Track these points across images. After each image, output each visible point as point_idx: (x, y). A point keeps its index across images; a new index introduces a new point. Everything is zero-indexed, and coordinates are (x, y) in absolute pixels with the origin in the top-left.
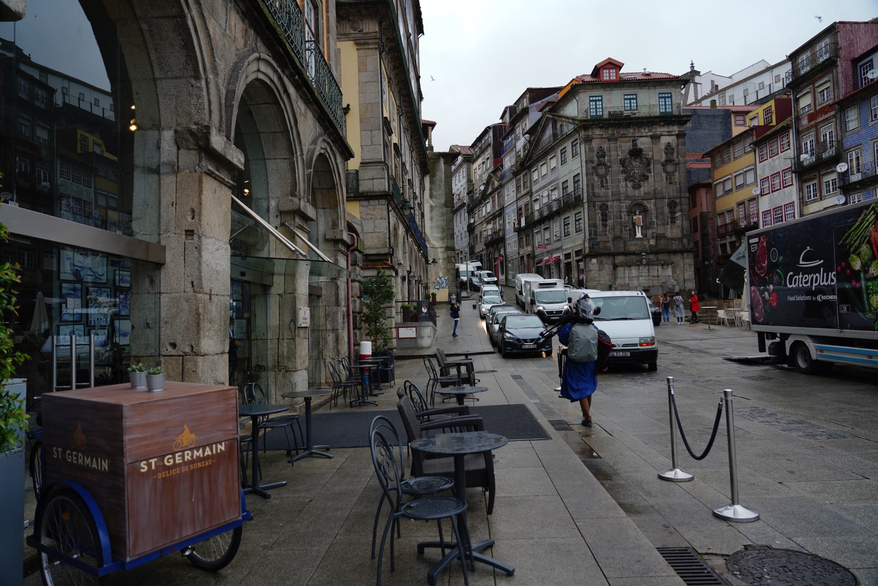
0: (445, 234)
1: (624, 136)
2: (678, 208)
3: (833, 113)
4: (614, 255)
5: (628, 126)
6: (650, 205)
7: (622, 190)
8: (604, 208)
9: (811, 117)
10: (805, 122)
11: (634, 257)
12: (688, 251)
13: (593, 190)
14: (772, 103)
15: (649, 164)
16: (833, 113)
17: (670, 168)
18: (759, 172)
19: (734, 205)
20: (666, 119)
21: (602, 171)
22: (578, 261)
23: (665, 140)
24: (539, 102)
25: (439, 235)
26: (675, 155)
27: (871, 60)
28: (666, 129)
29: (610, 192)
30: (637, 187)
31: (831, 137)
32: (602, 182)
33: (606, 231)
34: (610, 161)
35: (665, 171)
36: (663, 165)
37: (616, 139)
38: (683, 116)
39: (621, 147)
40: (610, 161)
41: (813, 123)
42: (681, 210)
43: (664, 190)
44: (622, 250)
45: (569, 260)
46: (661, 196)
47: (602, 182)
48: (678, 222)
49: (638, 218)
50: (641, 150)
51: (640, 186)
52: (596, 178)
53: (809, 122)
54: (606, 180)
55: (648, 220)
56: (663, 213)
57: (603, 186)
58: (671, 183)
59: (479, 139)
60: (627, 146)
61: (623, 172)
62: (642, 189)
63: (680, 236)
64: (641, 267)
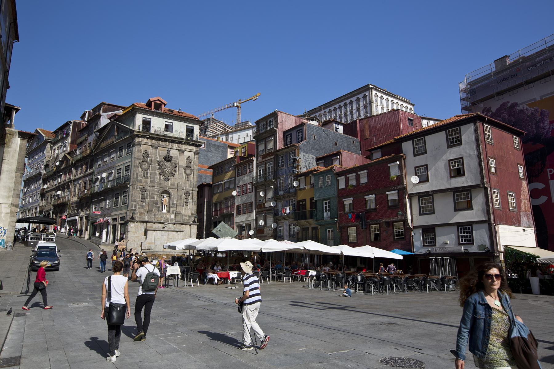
0: (11, 194)
1: (162, 146)
2: (191, 196)
3: (273, 157)
4: (146, 222)
5: (166, 140)
6: (173, 192)
7: (157, 180)
8: (143, 190)
9: (264, 157)
10: (260, 159)
11: (160, 225)
12: (194, 225)
13: (137, 177)
14: (246, 145)
15: (176, 167)
16: (273, 157)
17: (188, 172)
18: (237, 182)
19: (223, 199)
21: (145, 166)
22: (121, 224)
23: (187, 154)
24: (110, 113)
25: (6, 194)
26: (192, 164)
27: (291, 134)
30: (166, 180)
31: (272, 169)
32: (144, 173)
33: (143, 206)
35: (185, 173)
38: (198, 142)
39: (159, 153)
41: (264, 160)
42: (192, 198)
43: (183, 185)
44: (152, 220)
45: (115, 223)
46: (181, 188)
47: (144, 173)
48: (190, 205)
49: (166, 199)
50: (172, 157)
52: (140, 170)
53: (263, 159)
55: (171, 202)
56: (181, 199)
59: (61, 129)
60: (165, 153)
61: (158, 169)
62: (170, 181)
64: (163, 232)
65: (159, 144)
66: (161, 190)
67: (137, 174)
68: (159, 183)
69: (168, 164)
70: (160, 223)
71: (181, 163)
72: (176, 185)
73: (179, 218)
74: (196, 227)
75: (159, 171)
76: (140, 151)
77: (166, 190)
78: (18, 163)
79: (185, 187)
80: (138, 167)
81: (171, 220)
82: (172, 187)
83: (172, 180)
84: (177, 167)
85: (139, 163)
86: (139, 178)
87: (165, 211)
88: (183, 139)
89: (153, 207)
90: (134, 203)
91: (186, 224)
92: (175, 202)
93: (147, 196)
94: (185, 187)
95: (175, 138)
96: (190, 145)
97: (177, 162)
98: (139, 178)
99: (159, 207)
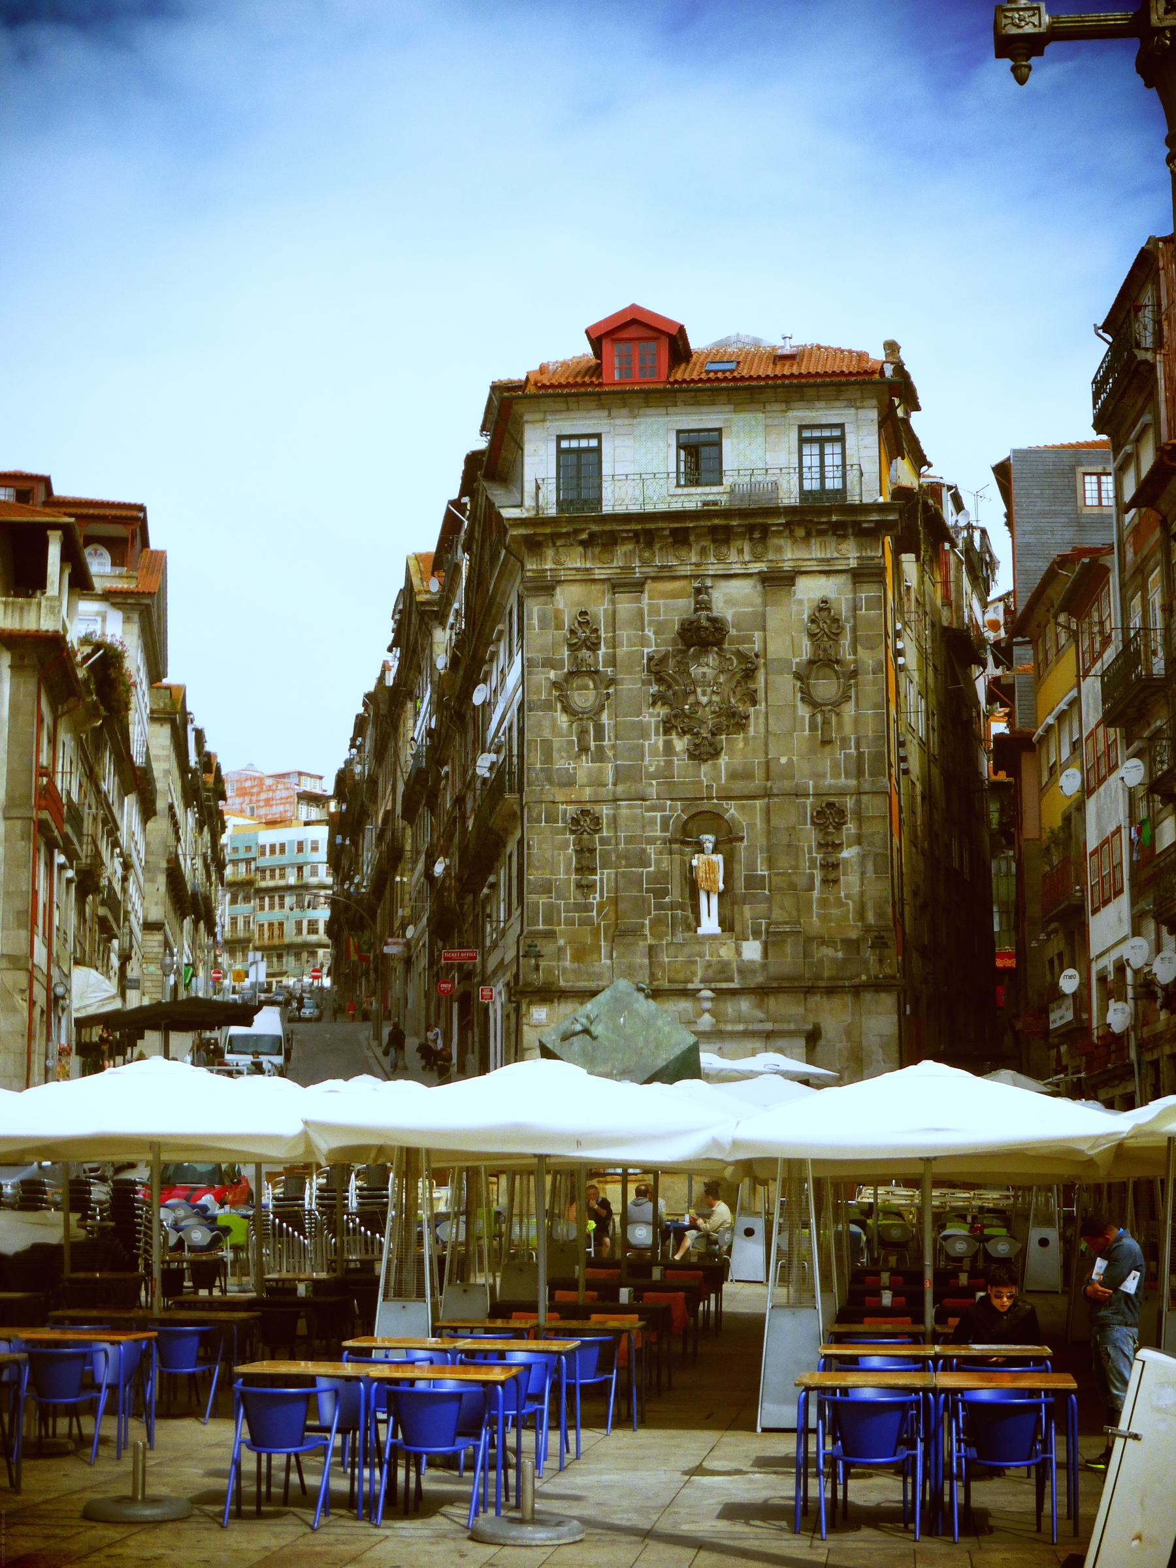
1: (666, 575)
2: (850, 827)
7: (652, 763)
8: (584, 823)
10: (1130, 555)
12: (877, 986)
13: (548, 758)
17: (825, 688)
19: (1058, 822)
20: (824, 515)
21: (584, 698)
23: (810, 590)
26: (846, 641)
28: (816, 551)
29: (609, 768)
30: (704, 752)
32: (583, 732)
33: (587, 908)
34: (612, 661)
35: (808, 698)
36: (798, 676)
37: (637, 587)
39: (654, 610)
40: (612, 661)
42: (859, 840)
46: (787, 785)
47: (583, 732)
48: (850, 882)
49: (709, 863)
51: (716, 754)
52: (563, 720)
54: (599, 729)
55: (741, 872)
56: (793, 849)
57: (584, 749)
58: (826, 742)
61: (656, 699)
62: (723, 760)
63: (853, 935)
65: (645, 563)
66: (677, 811)
67: (547, 747)
68: (665, 774)
69: (706, 668)
70: (685, 993)
71: (777, 648)
72: (759, 773)
73: (788, 960)
74: (888, 1001)
75: (662, 711)
76: (552, 621)
77: (706, 806)
78: (11, 772)
79: (818, 776)
80: (548, 706)
81: (745, 970)
82: (740, 786)
83: (736, 753)
84: (761, 676)
85: (555, 685)
86: (561, 763)
87: (710, 924)
88: (775, 511)
89: (640, 907)
90: (542, 900)
91: (831, 991)
92: (762, 871)
93: (605, 855)
94: (810, 778)
95: (727, 513)
96: (821, 533)
97: (757, 647)
98: (561, 763)
99: (673, 906)
